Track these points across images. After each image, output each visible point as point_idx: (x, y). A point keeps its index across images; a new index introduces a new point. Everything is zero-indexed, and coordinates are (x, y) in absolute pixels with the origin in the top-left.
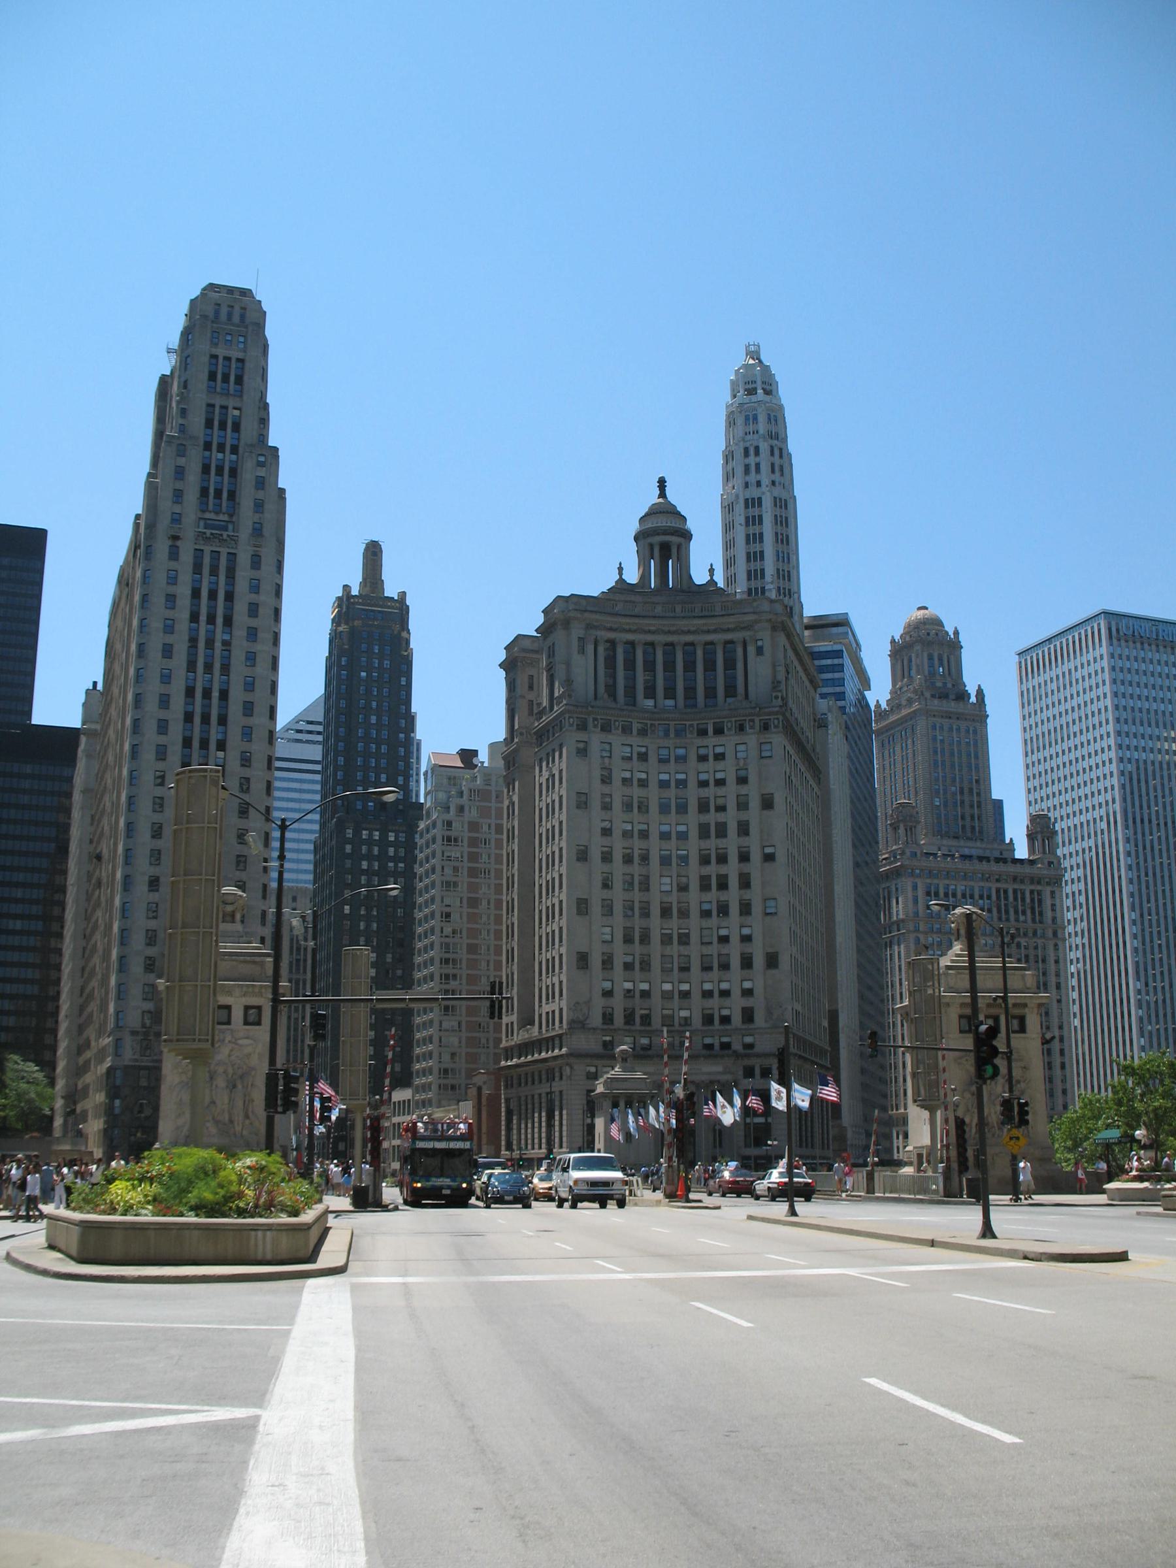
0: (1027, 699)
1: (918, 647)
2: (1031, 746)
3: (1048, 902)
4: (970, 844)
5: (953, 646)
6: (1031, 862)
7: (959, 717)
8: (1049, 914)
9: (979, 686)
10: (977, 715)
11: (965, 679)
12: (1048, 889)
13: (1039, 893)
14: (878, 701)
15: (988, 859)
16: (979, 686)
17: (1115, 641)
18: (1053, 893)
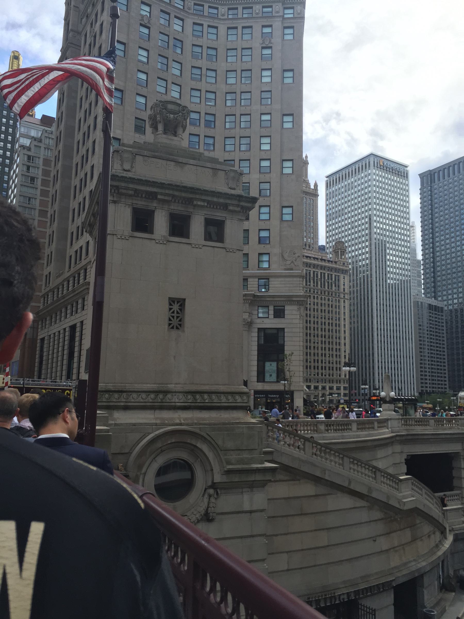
4: (309, 252)
7: (306, 193)
10: (314, 194)
15: (317, 259)
17: (376, 168)
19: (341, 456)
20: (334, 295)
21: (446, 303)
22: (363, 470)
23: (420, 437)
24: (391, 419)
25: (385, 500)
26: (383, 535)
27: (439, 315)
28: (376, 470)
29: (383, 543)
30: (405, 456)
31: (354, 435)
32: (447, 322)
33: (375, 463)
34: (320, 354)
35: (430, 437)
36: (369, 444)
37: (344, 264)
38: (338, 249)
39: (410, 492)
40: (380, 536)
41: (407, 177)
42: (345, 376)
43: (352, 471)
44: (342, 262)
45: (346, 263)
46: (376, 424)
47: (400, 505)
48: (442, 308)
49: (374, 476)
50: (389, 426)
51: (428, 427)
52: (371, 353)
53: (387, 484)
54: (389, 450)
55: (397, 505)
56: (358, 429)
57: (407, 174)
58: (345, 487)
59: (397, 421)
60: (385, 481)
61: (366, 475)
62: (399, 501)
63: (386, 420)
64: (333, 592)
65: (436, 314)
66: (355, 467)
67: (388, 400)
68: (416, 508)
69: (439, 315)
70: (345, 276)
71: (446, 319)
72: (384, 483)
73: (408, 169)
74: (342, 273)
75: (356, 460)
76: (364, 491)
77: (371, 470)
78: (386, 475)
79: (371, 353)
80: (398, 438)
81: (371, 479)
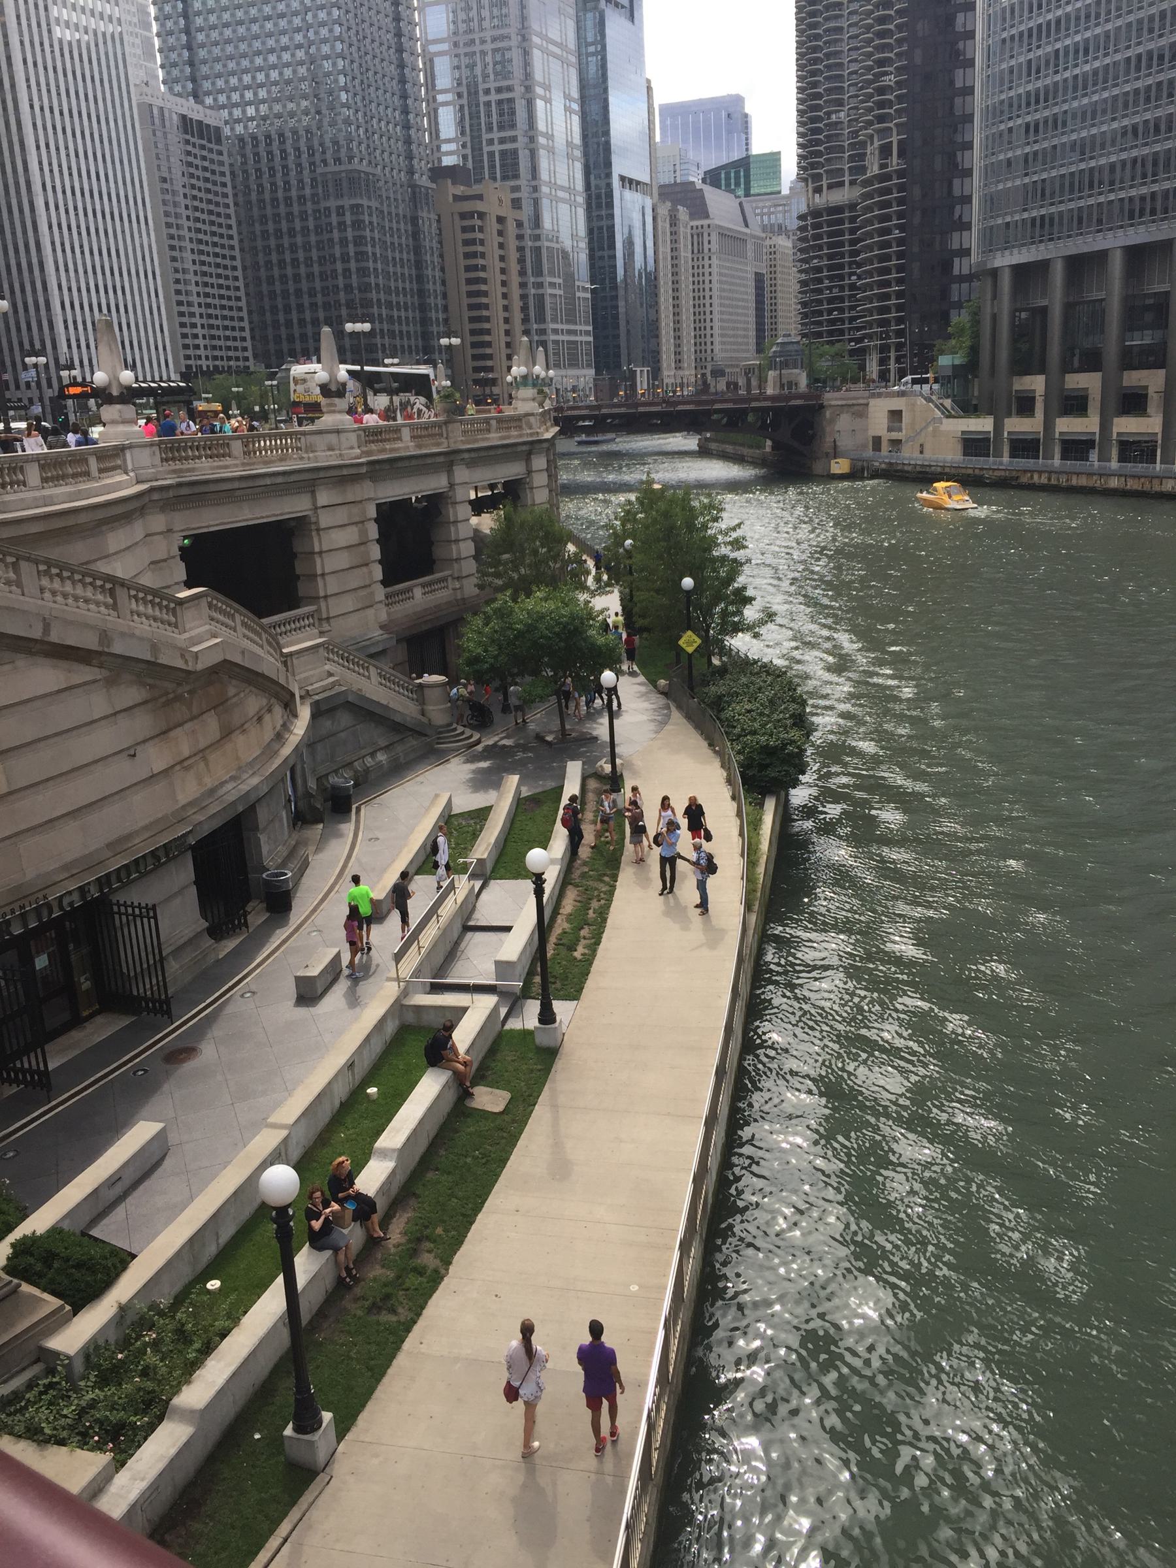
19: (10, 559)
21: (225, 113)
22: (79, 591)
23: (212, 488)
24: (131, 447)
25: (148, 656)
26: (152, 738)
27: (211, 150)
28: (113, 585)
29: (156, 758)
30: (179, 540)
31: (35, 498)
32: (232, 173)
33: (103, 567)
35: (236, 485)
36: (82, 518)
39: (207, 627)
40: (144, 742)
43: (47, 595)
46: (93, 464)
47: (186, 662)
48: (218, 130)
49: (110, 601)
50: (130, 467)
51: (228, 461)
52: (35, 260)
53: (147, 618)
54: (138, 530)
55: (179, 664)
56: (45, 480)
58: (36, 641)
59: (147, 451)
60: (141, 608)
61: (87, 601)
62: (183, 653)
63: (120, 450)
64: (40, 895)
65: (203, 147)
66: (57, 584)
67: (115, 392)
68: (225, 661)
71: (231, 165)
72: (139, 615)
75: (56, 566)
76: (89, 641)
77: (102, 587)
78: (141, 595)
79: (35, 260)
80: (156, 496)
81: (102, 609)
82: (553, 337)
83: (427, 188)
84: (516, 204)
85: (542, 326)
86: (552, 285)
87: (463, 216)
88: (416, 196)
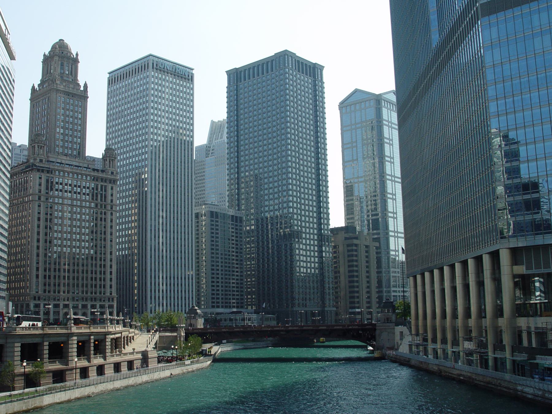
0: (111, 95)
1: (56, 58)
2: (111, 118)
3: (109, 192)
5: (75, 61)
6: (103, 171)
7: (73, 95)
8: (109, 198)
9: (86, 82)
11: (79, 78)
12: (109, 186)
13: (106, 187)
14: (34, 85)
16: (86, 82)
17: (155, 70)
18: (112, 188)
20: (99, 207)
27: (237, 225)
34: (80, 271)
37: (112, 173)
38: (107, 157)
41: (192, 81)
42: (111, 294)
44: (110, 171)
45: (115, 172)
52: (144, 268)
57: (192, 77)
69: (237, 225)
70: (114, 185)
73: (194, 72)
74: (110, 183)
79: (144, 268)
82: (393, 294)
83: (328, 236)
84: (377, 240)
85: (388, 289)
86: (395, 272)
87: (348, 246)
88: (322, 239)
